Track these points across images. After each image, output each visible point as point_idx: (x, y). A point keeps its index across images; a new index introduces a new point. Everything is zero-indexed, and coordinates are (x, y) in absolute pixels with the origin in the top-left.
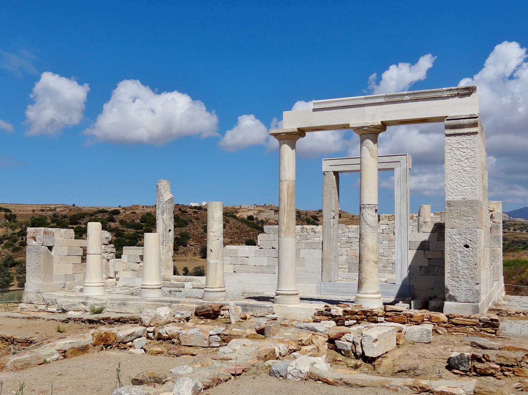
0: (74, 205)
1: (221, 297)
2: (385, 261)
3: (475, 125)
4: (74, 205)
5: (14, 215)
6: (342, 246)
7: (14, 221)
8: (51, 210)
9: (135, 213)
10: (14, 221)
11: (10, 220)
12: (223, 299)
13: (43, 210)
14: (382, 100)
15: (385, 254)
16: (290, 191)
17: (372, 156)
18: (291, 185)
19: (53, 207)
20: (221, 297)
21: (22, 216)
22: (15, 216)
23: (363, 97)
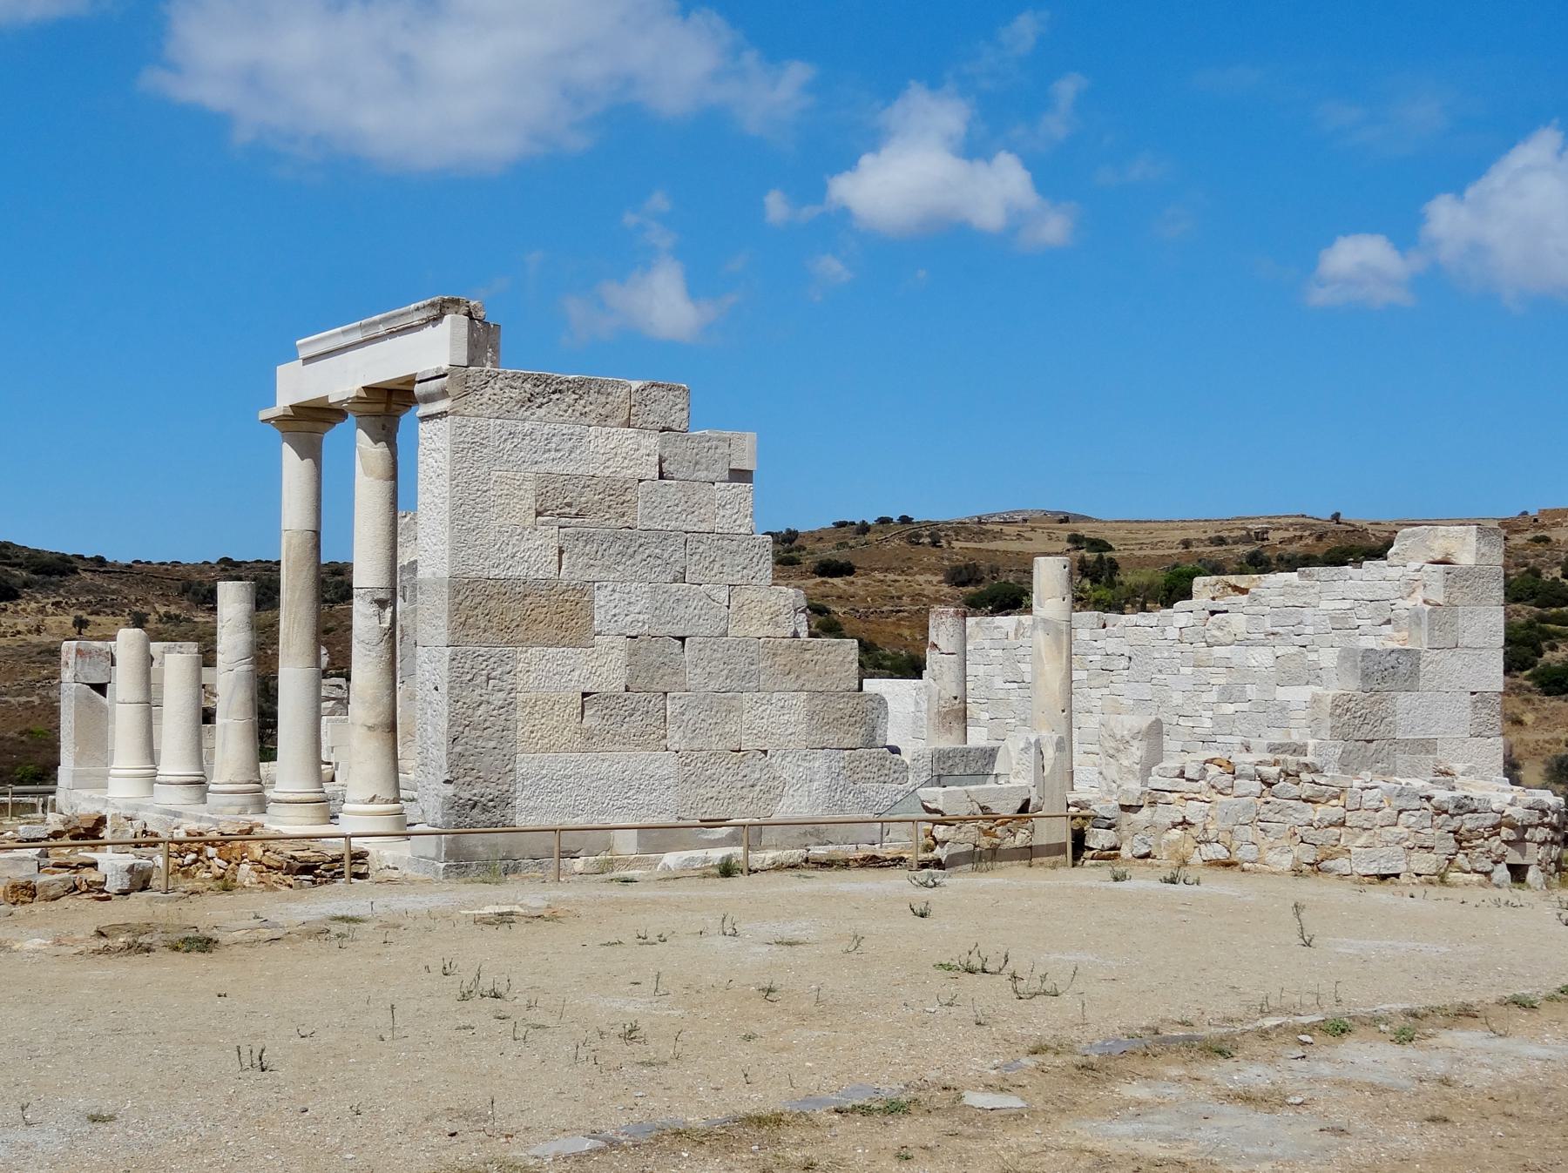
0: (1336, 517)
1: (230, 805)
2: (1187, 731)
3: (443, 394)
4: (1336, 517)
5: (1111, 560)
6: (1093, 683)
7: (1111, 584)
8: (1247, 540)
9: (1547, 540)
10: (1111, 584)
11: (1095, 581)
12: (236, 809)
13: (1220, 541)
14: (358, 337)
15: (1188, 710)
16: (292, 555)
17: (367, 472)
18: (295, 541)
19: (1255, 526)
20: (230, 805)
21: (1142, 562)
22: (1114, 566)
23: (339, 329)
